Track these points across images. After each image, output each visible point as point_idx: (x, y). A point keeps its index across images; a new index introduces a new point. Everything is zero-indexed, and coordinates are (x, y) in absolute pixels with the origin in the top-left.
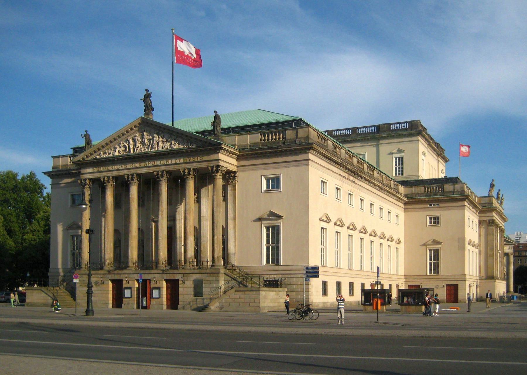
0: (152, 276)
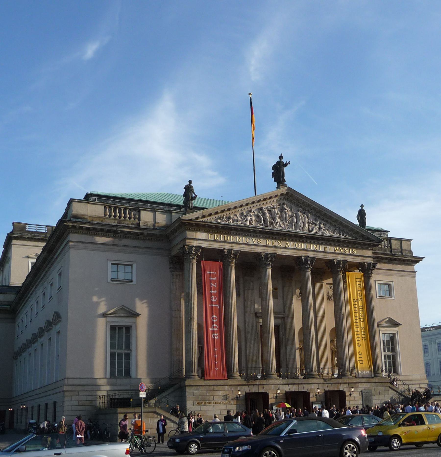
0: (310, 386)
